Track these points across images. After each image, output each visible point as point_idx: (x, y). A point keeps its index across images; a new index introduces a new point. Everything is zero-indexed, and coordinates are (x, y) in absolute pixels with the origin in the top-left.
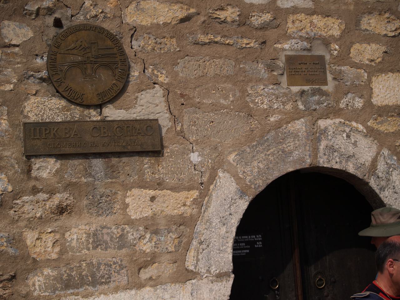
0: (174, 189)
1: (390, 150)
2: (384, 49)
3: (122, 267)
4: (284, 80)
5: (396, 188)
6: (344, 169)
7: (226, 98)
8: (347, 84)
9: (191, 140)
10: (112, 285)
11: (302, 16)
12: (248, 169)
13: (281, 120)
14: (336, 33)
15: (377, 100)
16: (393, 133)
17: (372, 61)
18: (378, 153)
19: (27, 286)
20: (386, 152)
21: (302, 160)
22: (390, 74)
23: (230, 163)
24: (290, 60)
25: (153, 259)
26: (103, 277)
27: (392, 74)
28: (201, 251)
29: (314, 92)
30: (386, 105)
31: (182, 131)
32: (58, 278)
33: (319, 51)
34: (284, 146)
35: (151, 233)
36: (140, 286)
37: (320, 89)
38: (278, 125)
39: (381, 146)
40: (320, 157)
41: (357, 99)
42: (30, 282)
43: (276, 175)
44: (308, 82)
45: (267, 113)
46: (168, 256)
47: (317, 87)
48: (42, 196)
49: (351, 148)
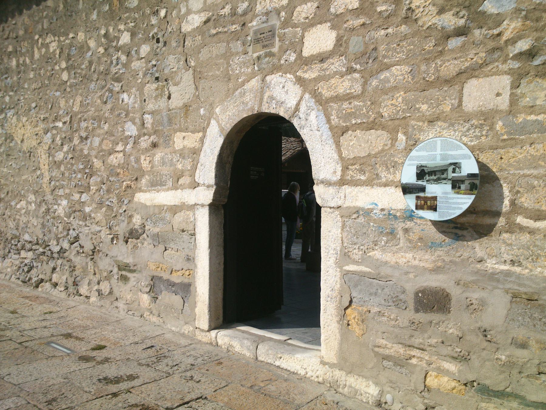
1: (310, 94)
2: (316, 5)
5: (312, 126)
10: (167, 187)
15: (306, 53)
16: (314, 78)
18: (301, 98)
20: (307, 96)
21: (252, 109)
22: (319, 26)
29: (266, 57)
31: (198, 95)
32: (149, 181)
36: (176, 189)
37: (270, 52)
40: (264, 105)
41: (292, 54)
43: (238, 119)
45: (238, 77)
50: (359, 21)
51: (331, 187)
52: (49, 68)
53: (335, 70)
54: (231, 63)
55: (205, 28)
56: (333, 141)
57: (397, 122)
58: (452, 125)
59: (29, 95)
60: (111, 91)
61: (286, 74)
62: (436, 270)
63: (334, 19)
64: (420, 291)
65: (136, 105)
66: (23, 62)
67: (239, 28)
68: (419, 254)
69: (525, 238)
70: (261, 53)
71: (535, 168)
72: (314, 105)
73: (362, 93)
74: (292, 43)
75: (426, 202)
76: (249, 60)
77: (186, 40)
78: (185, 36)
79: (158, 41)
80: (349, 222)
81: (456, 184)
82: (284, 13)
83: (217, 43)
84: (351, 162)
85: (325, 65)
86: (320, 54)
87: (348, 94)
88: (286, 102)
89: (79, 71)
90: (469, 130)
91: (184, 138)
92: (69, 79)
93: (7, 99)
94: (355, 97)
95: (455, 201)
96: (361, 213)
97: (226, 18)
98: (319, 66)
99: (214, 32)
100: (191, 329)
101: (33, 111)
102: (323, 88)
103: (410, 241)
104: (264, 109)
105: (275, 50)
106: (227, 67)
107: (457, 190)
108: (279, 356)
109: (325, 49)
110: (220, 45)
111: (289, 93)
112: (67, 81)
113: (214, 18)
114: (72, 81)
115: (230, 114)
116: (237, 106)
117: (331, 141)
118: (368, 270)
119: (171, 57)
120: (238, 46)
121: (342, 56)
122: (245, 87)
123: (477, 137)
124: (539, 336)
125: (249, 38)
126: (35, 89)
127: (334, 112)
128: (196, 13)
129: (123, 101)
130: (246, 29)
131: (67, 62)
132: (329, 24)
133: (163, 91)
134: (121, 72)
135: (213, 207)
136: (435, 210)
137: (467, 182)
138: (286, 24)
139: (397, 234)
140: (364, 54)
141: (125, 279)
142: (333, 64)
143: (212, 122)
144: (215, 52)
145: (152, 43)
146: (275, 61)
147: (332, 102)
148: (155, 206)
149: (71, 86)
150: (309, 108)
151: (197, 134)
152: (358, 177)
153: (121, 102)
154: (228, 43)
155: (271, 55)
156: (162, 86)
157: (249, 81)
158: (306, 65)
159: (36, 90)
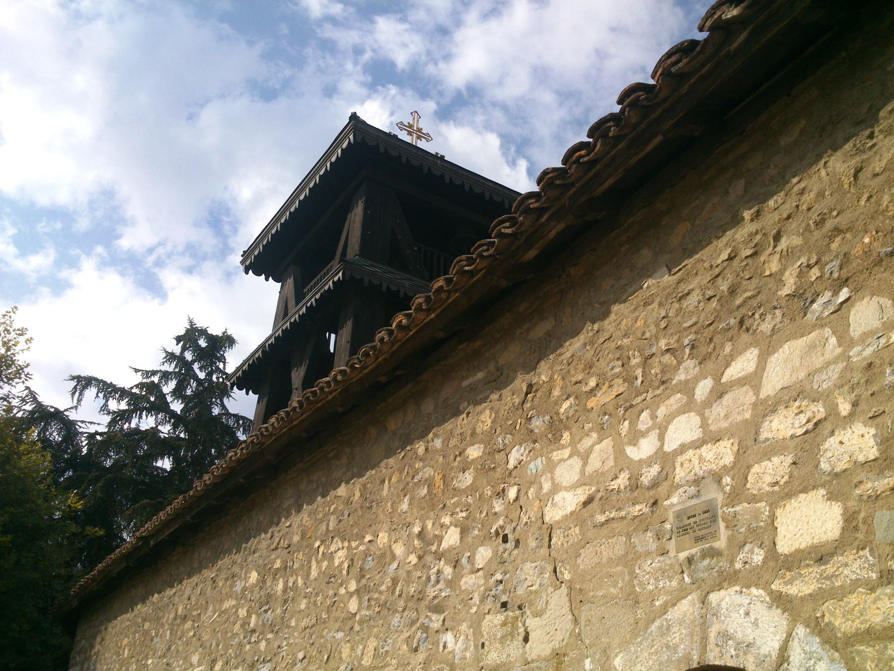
1: (807, 626)
2: (789, 459)
4: (672, 546)
6: (742, 666)
8: (741, 530)
11: (690, 453)
15: (784, 546)
16: (810, 595)
17: (777, 483)
18: (789, 635)
20: (801, 631)
27: (805, 495)
29: (704, 556)
30: (796, 550)
31: (579, 634)
34: (669, 639)
37: (711, 548)
40: (711, 650)
41: (756, 550)
47: (707, 546)
50: (886, 481)
52: (331, 593)
53: (854, 577)
54: (638, 571)
55: (585, 513)
59: (296, 638)
60: (425, 629)
61: (748, 587)
63: (831, 482)
65: (468, 655)
66: (294, 583)
67: (646, 510)
70: (693, 551)
74: (752, 531)
76: (671, 566)
77: (553, 535)
78: (551, 528)
79: (505, 539)
82: (729, 479)
83: (609, 538)
85: (830, 569)
86: (813, 548)
88: (758, 643)
89: (376, 596)
92: (359, 610)
93: (263, 644)
97: (621, 494)
98: (816, 570)
99: (601, 518)
101: (299, 665)
102: (833, 614)
104: (711, 658)
105: (721, 543)
106: (631, 580)
109: (824, 538)
110: (614, 540)
111: (760, 625)
112: (356, 614)
113: (600, 495)
114: (363, 613)
116: (656, 652)
119: (528, 565)
120: (649, 541)
121: (862, 549)
122: (668, 616)
125: (668, 526)
126: (305, 628)
128: (568, 489)
129: (444, 647)
130: (659, 511)
131: (358, 582)
132: (822, 492)
133: (514, 627)
134: (443, 594)
138: (736, 496)
142: (846, 565)
144: (606, 554)
145: (495, 544)
146: (724, 564)
147: (861, 642)
149: (361, 622)
150: (809, 656)
153: (441, 648)
154: (629, 536)
155: (713, 553)
156: (513, 618)
157: (675, 604)
158: (789, 569)
159: (308, 630)
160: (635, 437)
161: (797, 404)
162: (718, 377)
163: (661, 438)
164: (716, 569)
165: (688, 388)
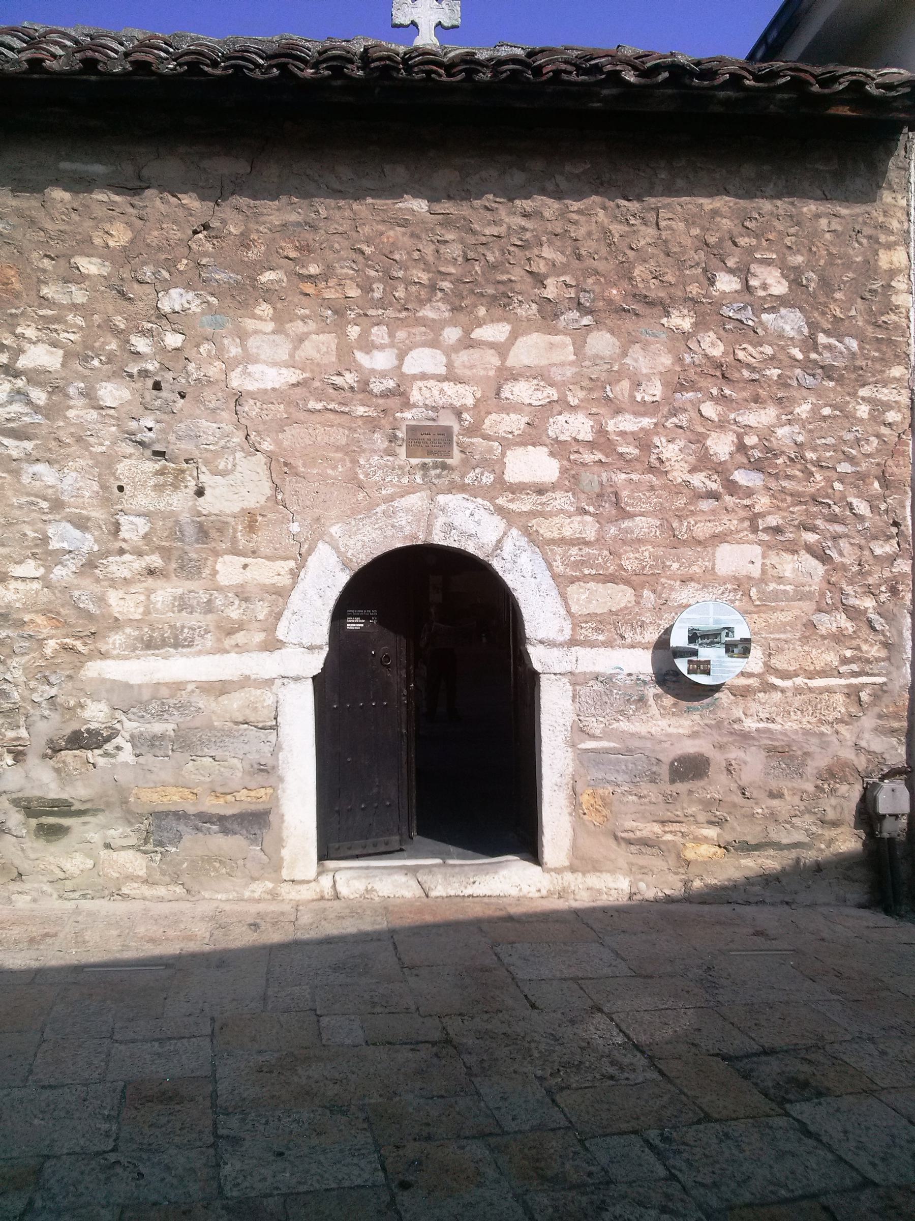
0: (268, 558)
2: (526, 419)
3: (207, 632)
7: (335, 468)
9: (292, 510)
11: (431, 383)
12: (351, 542)
13: (396, 493)
14: (470, 401)
18: (505, 534)
19: (107, 643)
20: (514, 532)
22: (530, 447)
23: (332, 535)
24: (412, 429)
25: (240, 627)
26: (185, 640)
28: (293, 621)
29: (435, 466)
33: (447, 420)
35: (241, 600)
38: (391, 498)
39: (510, 525)
41: (486, 474)
42: (111, 641)
44: (430, 453)
46: (258, 625)
48: (127, 557)
49: (472, 526)
51: (555, 649)
56: (557, 592)
57: (643, 578)
58: (705, 586)
62: (694, 735)
64: (676, 760)
68: (674, 721)
69: (777, 696)
71: (785, 632)
72: (526, 546)
73: (597, 540)
75: (699, 666)
79: (157, 386)
80: (583, 691)
81: (730, 648)
84: (585, 619)
85: (544, 499)
86: (535, 484)
87: (578, 538)
90: (723, 593)
91: (245, 566)
94: (587, 543)
95: (728, 664)
96: (601, 679)
98: (534, 497)
100: (270, 885)
103: (664, 708)
107: (730, 654)
108: (472, 880)
115: (365, 538)
116: (381, 528)
117: (554, 593)
118: (612, 745)
123: (733, 602)
124: (790, 785)
127: (558, 557)
132: (545, 449)
134: (27, 419)
135: (321, 683)
136: (709, 674)
137: (740, 647)
138: (474, 430)
139: (648, 700)
140: (600, 496)
141: (52, 833)
143: (320, 545)
145: (139, 385)
148: (158, 683)
151: (282, 563)
152: (594, 637)
155: (444, 467)
156: (174, 469)
157: (403, 496)
158: (513, 493)
160: (369, 347)
161: (535, 382)
162: (467, 332)
163: (401, 357)
164: (448, 479)
165: (436, 327)
